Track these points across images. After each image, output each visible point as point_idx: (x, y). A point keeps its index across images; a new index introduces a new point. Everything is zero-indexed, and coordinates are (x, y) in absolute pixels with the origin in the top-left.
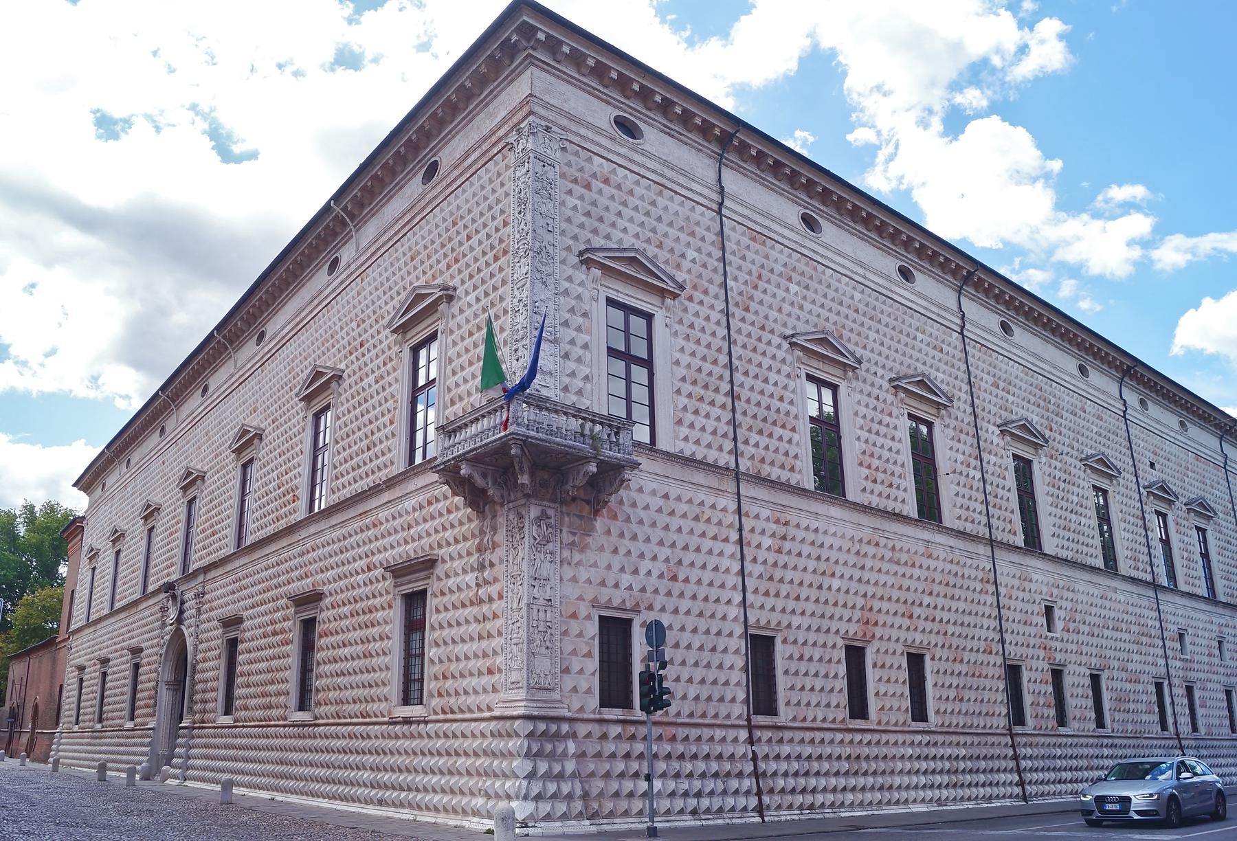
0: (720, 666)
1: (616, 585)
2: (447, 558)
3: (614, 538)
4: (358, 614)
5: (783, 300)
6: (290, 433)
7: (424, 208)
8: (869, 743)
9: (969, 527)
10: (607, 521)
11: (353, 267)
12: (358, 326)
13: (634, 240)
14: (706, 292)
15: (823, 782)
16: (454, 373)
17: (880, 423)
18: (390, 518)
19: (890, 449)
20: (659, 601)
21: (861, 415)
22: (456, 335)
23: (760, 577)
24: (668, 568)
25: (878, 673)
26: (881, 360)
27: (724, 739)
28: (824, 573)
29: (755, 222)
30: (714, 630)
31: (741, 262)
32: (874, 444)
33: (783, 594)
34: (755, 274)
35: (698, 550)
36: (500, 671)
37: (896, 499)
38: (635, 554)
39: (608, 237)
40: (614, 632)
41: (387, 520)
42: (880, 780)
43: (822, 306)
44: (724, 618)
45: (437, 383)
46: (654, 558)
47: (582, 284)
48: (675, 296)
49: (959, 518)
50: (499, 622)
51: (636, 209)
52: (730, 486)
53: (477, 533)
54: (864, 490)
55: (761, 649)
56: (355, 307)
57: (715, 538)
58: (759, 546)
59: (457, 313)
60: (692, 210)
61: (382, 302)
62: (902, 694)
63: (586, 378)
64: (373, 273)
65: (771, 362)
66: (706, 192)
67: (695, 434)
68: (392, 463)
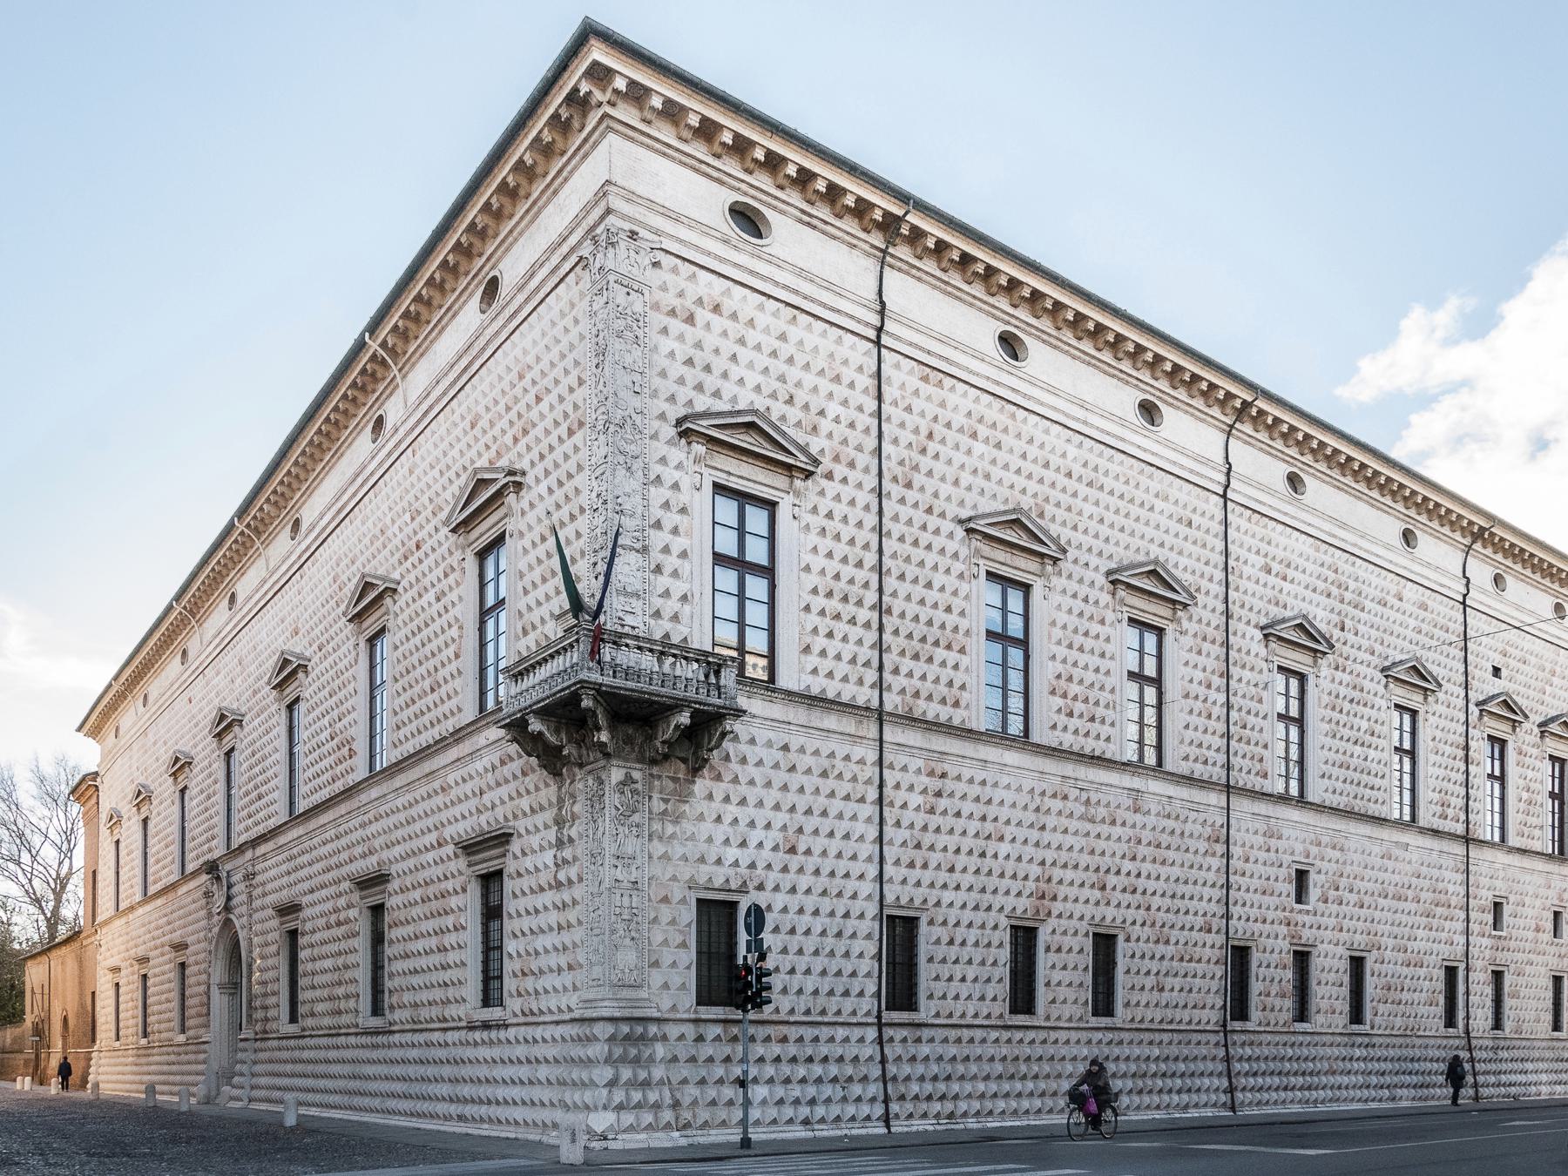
0: (847, 954)
1: (719, 862)
3: (716, 805)
9: (1199, 770)
10: (708, 782)
16: (526, 592)
20: (773, 878)
21: (1060, 624)
23: (904, 843)
24: (785, 838)
26: (1098, 544)
27: (846, 1040)
30: (840, 912)
33: (933, 864)
35: (824, 813)
36: (581, 966)
37: (1098, 737)
38: (743, 823)
40: (718, 917)
44: (854, 896)
46: (768, 826)
49: (1186, 758)
52: (873, 731)
53: (554, 800)
54: (1054, 727)
55: (901, 935)
61: (438, 487)
65: (938, 558)
67: (827, 665)
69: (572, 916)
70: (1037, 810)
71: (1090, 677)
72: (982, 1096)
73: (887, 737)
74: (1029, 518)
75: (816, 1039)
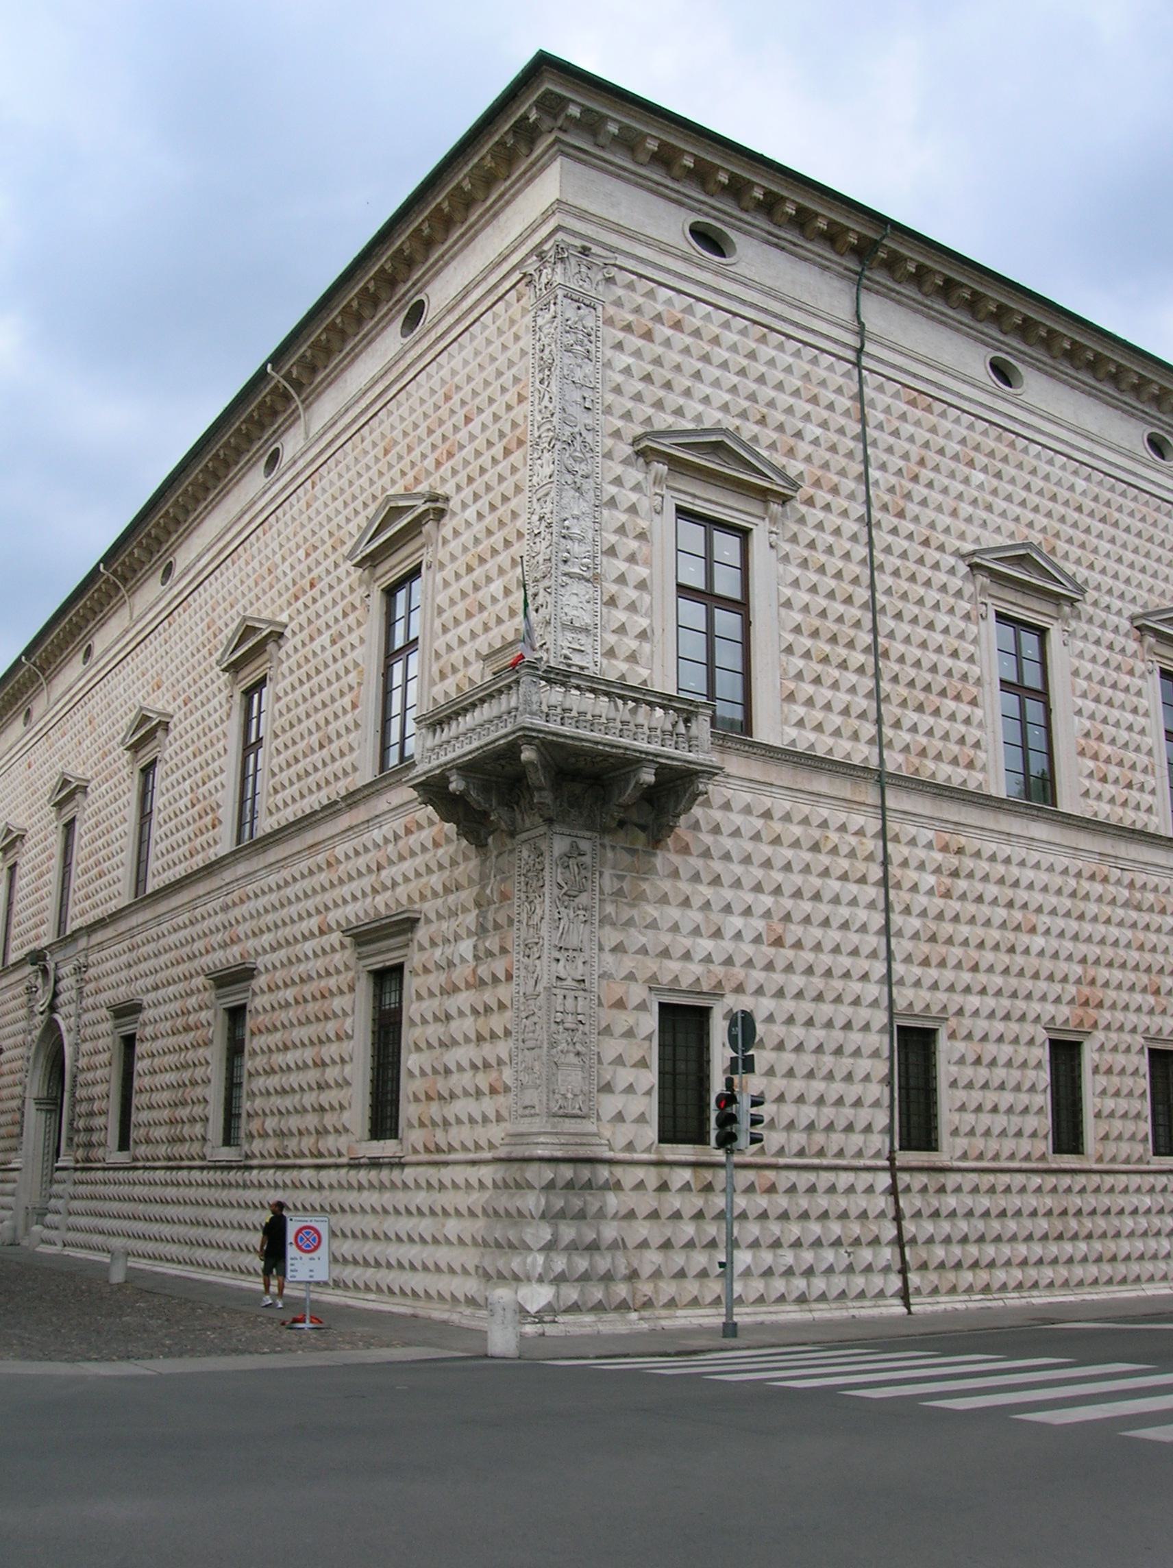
1: (687, 956)
2: (433, 916)
4: (305, 1001)
5: (960, 496)
6: (210, 721)
7: (403, 373)
8: (1083, 1190)
11: (301, 464)
12: (308, 555)
13: (719, 415)
14: (835, 490)
15: (1006, 1250)
16: (445, 629)
17: (1114, 686)
18: (351, 854)
19: (1130, 728)
21: (1083, 673)
22: (448, 573)
25: (1102, 1080)
26: (1120, 586)
27: (851, 1189)
28: (1018, 928)
29: (915, 376)
31: (891, 440)
32: (1105, 721)
33: (952, 962)
34: (915, 458)
36: (507, 1089)
39: (679, 412)
40: (683, 1024)
41: (347, 857)
42: (1098, 1246)
43: (1023, 503)
45: (420, 646)
47: (637, 488)
48: (785, 500)
50: (508, 1014)
51: (724, 365)
53: (476, 877)
54: (1086, 794)
56: (303, 526)
57: (844, 877)
58: (914, 888)
59: (449, 536)
60: (814, 361)
61: (341, 519)
62: (1138, 1116)
63: (643, 635)
64: (329, 475)
66: (835, 332)
68: (355, 769)
69: (497, 1022)
70: (1073, 894)
71: (1124, 735)
72: (1024, 1263)
73: (890, 803)
74: (1040, 553)
75: (812, 1189)
